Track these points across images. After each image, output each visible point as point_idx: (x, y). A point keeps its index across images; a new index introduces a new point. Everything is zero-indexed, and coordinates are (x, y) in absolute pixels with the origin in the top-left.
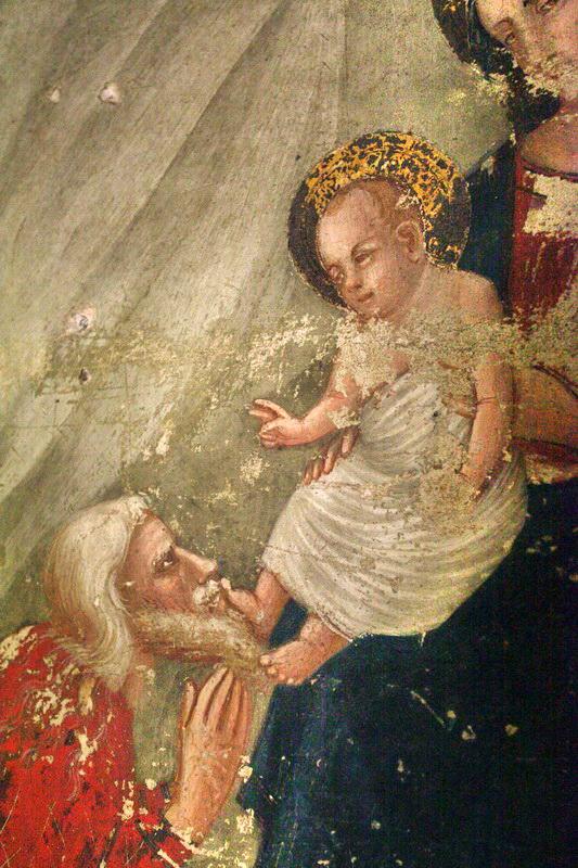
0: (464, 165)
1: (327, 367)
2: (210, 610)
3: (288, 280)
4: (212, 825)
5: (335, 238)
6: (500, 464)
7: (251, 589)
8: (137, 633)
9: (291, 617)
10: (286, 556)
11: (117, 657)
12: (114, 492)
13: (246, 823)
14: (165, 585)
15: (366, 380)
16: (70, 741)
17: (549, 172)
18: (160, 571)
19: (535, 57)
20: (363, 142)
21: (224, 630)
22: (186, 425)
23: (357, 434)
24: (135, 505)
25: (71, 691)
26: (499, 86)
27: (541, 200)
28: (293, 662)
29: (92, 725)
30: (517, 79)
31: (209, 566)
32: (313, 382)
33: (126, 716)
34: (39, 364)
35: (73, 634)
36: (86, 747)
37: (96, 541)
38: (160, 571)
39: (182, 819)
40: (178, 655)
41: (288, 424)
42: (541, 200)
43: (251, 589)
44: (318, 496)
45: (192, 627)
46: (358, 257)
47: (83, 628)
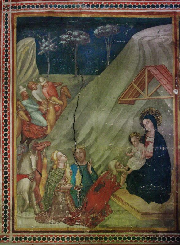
0: (142, 135)
1: (132, 150)
2: (122, 168)
3: (128, 143)
4: (123, 184)
5: (132, 140)
6: (144, 157)
7: (126, 167)
8: (116, 171)
9: (129, 169)
10: (129, 164)
11: (115, 172)
12: (114, 159)
13: (126, 184)
14: (119, 167)
15: (135, 151)
16: (111, 179)
17: (148, 136)
18: (118, 166)
19: (147, 128)
20: (135, 132)
21: (124, 170)
22: (120, 154)
23: (134, 155)
24: (116, 160)
25: (111, 175)
26: (144, 129)
27: (147, 138)
28: (129, 172)
29: (113, 178)
30: (146, 129)
31: (123, 165)
32: (131, 151)
33: (116, 177)
34: (106, 148)
35: (111, 171)
36: (112, 180)
37: (112, 164)
38: (118, 166)
39: (121, 184)
40: (120, 172)
41: (129, 154)
42: (147, 138)
43: (126, 167)
44: (131, 160)
45: (121, 170)
46: (134, 142)
47: (112, 171)
